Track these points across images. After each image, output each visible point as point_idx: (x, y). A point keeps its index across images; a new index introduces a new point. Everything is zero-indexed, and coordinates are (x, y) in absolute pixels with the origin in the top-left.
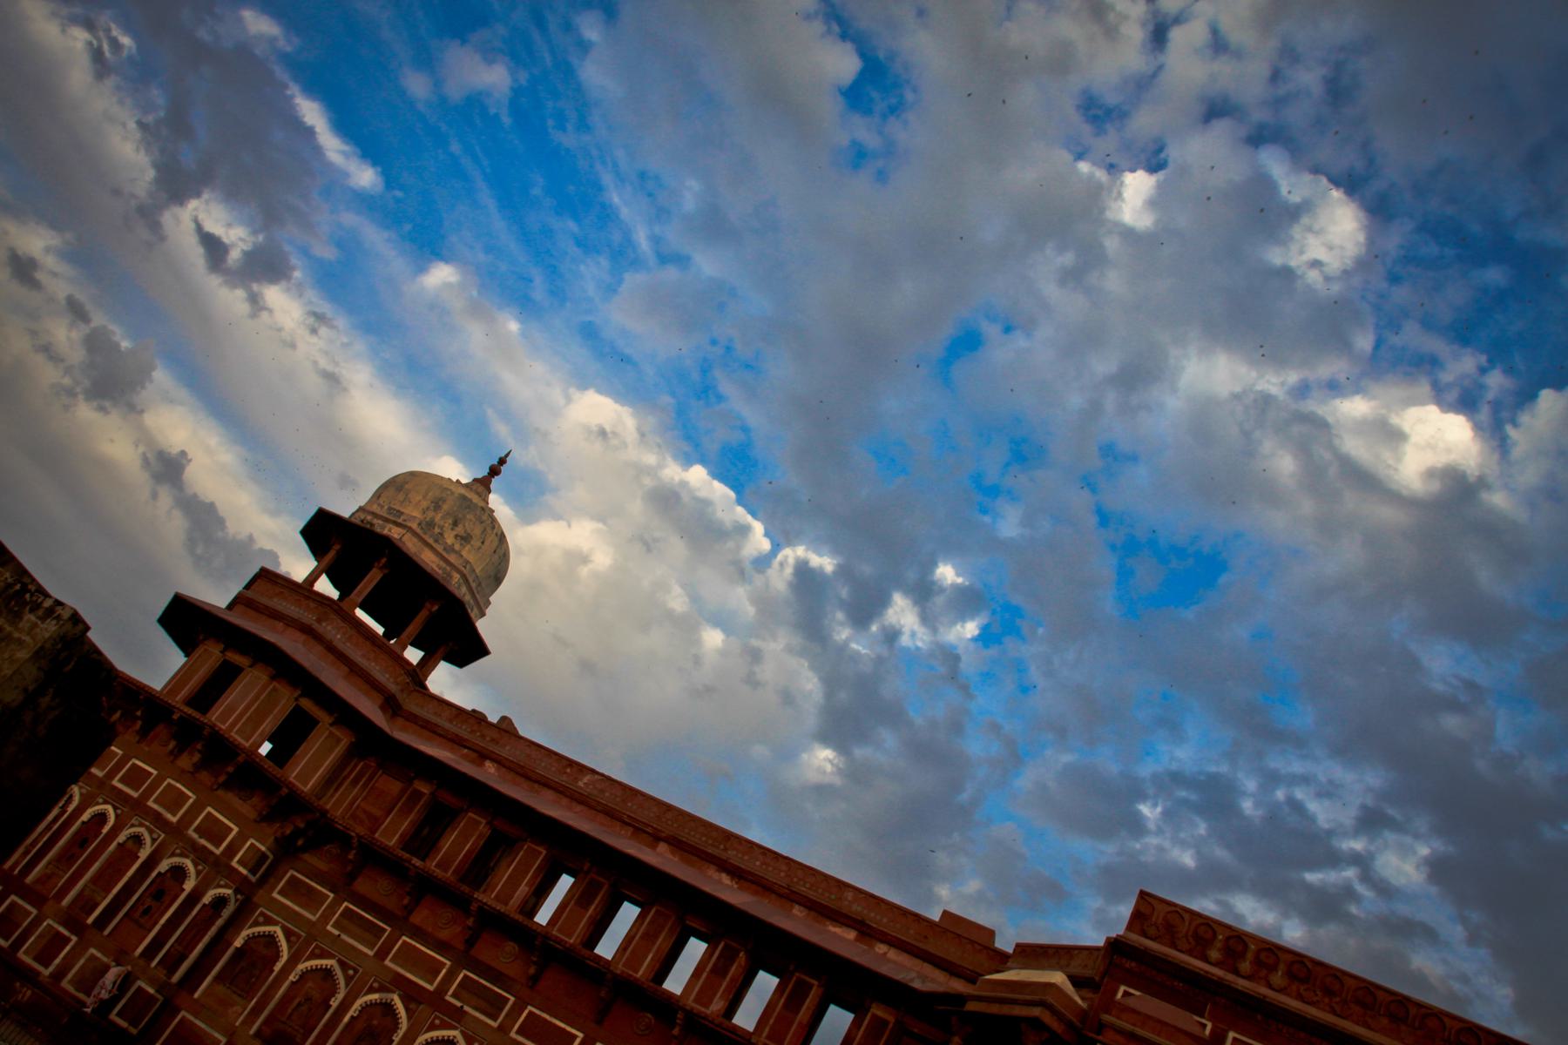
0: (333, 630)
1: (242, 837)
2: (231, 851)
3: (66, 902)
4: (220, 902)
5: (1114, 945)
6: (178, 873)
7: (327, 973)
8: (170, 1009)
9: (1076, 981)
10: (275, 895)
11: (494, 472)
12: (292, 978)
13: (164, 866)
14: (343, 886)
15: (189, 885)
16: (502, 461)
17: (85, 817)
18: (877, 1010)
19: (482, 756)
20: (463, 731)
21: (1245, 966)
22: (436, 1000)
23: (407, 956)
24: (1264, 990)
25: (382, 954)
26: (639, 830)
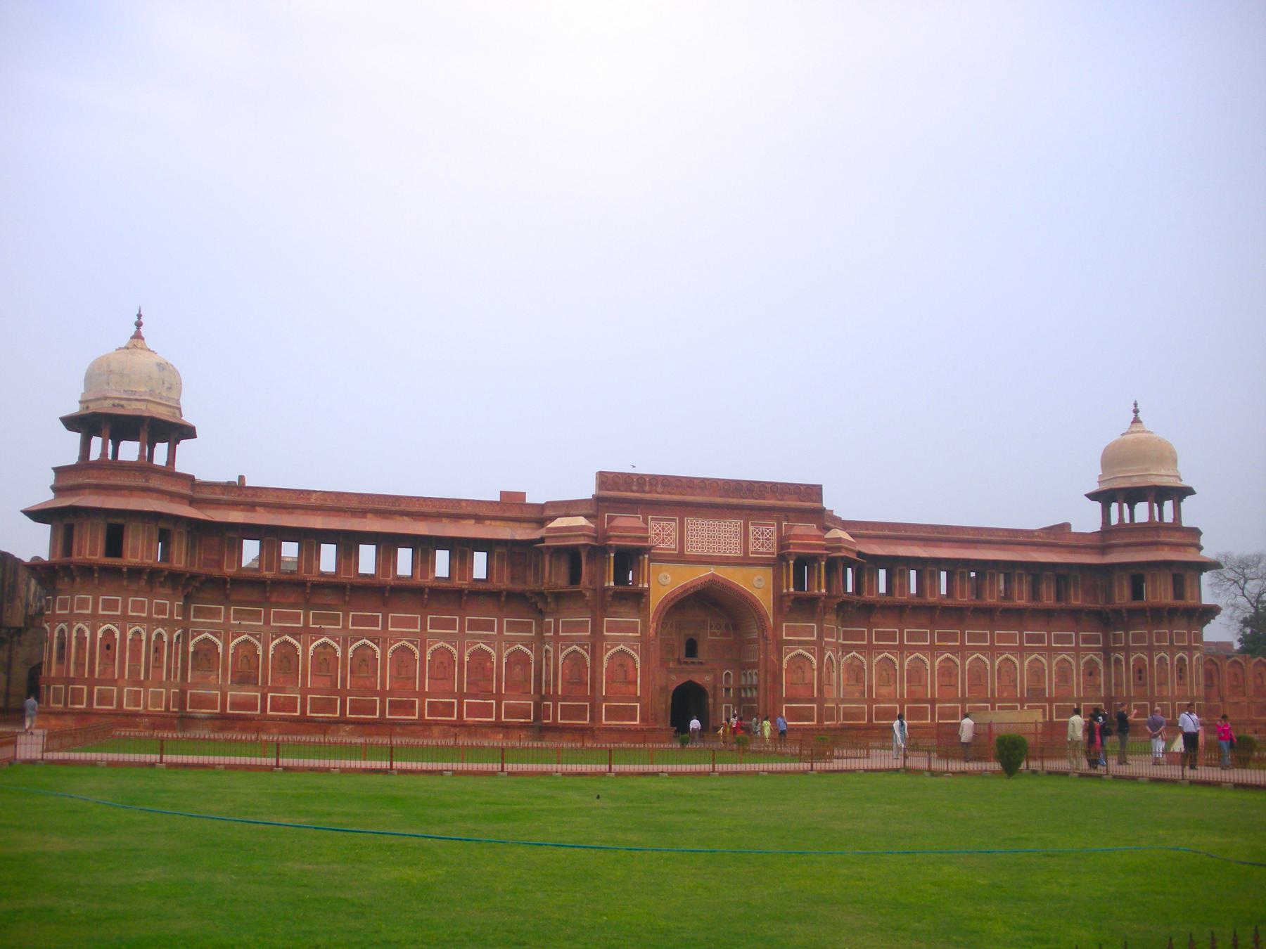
4: (178, 637)
5: (597, 499)
6: (160, 636)
7: (246, 641)
11: (139, 325)
12: (231, 652)
13: (153, 638)
14: (227, 600)
15: (166, 639)
16: (139, 316)
17: (100, 635)
18: (498, 550)
19: (252, 507)
21: (647, 488)
22: (306, 628)
23: (279, 617)
24: (655, 496)
25: (267, 622)
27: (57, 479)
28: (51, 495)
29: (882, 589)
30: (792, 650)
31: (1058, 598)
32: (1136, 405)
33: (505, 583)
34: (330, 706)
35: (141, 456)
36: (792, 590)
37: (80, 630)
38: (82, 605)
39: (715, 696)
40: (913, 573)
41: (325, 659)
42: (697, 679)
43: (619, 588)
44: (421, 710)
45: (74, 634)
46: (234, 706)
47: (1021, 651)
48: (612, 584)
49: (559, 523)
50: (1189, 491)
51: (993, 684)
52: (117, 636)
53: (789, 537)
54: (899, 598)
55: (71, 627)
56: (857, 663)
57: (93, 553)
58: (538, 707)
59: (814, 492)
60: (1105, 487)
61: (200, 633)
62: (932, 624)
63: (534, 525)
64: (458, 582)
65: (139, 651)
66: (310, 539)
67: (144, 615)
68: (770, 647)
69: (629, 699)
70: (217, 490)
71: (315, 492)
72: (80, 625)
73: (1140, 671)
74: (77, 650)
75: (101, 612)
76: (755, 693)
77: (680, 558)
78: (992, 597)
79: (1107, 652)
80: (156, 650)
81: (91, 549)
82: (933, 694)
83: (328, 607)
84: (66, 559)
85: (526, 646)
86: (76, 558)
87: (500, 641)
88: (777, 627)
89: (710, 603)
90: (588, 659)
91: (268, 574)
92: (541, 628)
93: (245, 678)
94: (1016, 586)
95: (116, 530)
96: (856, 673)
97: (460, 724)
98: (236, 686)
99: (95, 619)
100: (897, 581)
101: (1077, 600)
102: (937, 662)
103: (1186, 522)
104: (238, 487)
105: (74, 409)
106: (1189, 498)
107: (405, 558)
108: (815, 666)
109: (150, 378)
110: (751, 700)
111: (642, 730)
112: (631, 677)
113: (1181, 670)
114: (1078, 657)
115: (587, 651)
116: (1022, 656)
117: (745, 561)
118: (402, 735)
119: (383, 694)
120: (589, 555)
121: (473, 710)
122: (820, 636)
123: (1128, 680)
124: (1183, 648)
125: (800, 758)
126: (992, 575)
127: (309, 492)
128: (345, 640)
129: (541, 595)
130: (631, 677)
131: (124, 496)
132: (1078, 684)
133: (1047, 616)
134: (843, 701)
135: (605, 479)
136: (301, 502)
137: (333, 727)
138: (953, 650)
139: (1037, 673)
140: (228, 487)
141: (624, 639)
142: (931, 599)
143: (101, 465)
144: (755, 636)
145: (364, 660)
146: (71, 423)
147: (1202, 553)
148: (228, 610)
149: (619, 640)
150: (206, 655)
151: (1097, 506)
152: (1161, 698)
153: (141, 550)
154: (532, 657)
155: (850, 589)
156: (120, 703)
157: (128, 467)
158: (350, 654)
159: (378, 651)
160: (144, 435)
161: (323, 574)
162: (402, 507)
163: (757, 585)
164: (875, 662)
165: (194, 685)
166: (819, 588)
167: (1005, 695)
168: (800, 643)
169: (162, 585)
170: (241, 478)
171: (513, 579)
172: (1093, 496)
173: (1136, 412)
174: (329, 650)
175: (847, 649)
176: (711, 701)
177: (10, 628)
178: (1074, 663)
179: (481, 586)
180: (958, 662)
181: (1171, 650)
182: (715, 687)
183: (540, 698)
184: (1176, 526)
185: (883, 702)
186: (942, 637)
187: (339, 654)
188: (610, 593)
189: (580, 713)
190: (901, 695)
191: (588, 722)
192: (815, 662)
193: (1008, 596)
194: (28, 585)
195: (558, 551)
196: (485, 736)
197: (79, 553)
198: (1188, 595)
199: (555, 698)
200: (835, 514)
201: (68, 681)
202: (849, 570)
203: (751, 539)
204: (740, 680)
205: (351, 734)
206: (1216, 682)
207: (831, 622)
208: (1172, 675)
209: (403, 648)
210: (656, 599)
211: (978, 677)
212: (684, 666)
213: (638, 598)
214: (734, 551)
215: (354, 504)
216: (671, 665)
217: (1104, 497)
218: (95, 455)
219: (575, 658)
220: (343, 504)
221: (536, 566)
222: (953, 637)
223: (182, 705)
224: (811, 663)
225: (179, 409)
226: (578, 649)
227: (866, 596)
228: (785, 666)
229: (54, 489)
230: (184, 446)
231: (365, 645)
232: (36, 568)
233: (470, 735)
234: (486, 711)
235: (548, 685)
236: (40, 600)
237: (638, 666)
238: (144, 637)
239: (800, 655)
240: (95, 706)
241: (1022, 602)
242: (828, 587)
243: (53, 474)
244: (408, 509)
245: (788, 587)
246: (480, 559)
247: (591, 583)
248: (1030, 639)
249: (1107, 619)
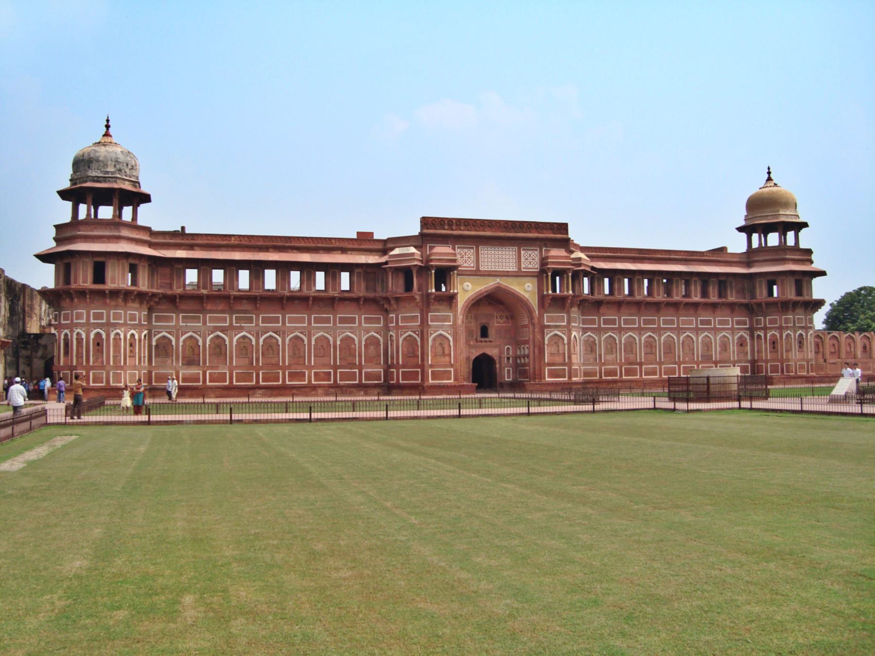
0: (125, 233)
1: (140, 314)
2: (140, 320)
3: (112, 364)
5: (421, 235)
6: (133, 335)
7: (191, 337)
8: (150, 373)
9: (415, 247)
10: (154, 324)
11: (108, 127)
12: (181, 344)
13: (128, 337)
14: (176, 309)
15: (137, 337)
16: (108, 121)
17: (92, 336)
18: (357, 270)
19: (191, 247)
20: (178, 241)
21: (454, 227)
22: (231, 326)
23: (212, 320)
25: (205, 323)
26: (261, 249)
27: (57, 234)
28: (54, 244)
29: (607, 292)
30: (551, 332)
31: (720, 296)
32: (769, 168)
33: (361, 292)
34: (247, 377)
35: (114, 216)
36: (550, 292)
37: (78, 334)
38: (79, 316)
40: (626, 280)
41: (244, 347)
43: (438, 293)
44: (310, 378)
45: (75, 336)
46: (184, 380)
47: (697, 330)
48: (434, 290)
49: (397, 251)
50: (805, 225)
51: (679, 351)
52: (104, 336)
53: (547, 258)
54: (617, 297)
55: (72, 332)
56: (591, 339)
57: (85, 281)
58: (384, 371)
59: (563, 228)
60: (750, 223)
61: (159, 332)
62: (639, 313)
63: (380, 253)
64: (331, 293)
65: (120, 346)
66: (231, 267)
67: (122, 322)
68: (536, 330)
69: (445, 366)
70: (167, 236)
71: (234, 235)
72: (79, 330)
73: (774, 343)
74: (77, 347)
75: (92, 321)
76: (527, 360)
77: (477, 273)
78: (677, 295)
79: (751, 330)
80: (131, 345)
81: (84, 279)
82: (641, 359)
83: (245, 312)
84: (66, 287)
85: (377, 333)
86: (73, 286)
87: (361, 330)
88: (541, 316)
89: (494, 301)
90: (419, 340)
91: (204, 292)
92: (387, 321)
93: (190, 362)
94: (693, 288)
95: (99, 265)
96: (591, 347)
97: (335, 386)
98: (185, 367)
99: (88, 326)
100: (616, 286)
101: (732, 298)
102: (643, 338)
103: (803, 245)
104: (181, 234)
105: (66, 185)
106: (804, 231)
107: (295, 277)
108: (566, 342)
109: (117, 161)
110: (524, 365)
111: (455, 386)
113: (800, 342)
114: (733, 334)
115: (418, 335)
116: (697, 334)
117: (519, 274)
118: (298, 395)
119: (284, 368)
120: (417, 272)
121: (344, 376)
122: (569, 322)
123: (766, 350)
124: (802, 328)
125: (576, 402)
126: (677, 281)
127: (230, 236)
128: (257, 334)
129: (387, 299)
130: (447, 351)
131: (104, 242)
132: (734, 352)
133: (714, 306)
134: (584, 364)
135: (426, 222)
136: (226, 242)
137: (251, 392)
138: (653, 330)
139: (707, 345)
140: (174, 234)
141: (441, 327)
142: (638, 298)
143: (87, 222)
144: (526, 322)
145: (271, 347)
146: (64, 194)
147: (813, 265)
148: (178, 316)
150: (163, 349)
151: (744, 236)
152: (788, 360)
153: (119, 278)
154: (381, 340)
155: (586, 290)
156: (108, 381)
157: (105, 223)
158: (261, 343)
159: (280, 340)
160: (116, 201)
161: (240, 291)
162: (293, 244)
163: (527, 290)
164: (603, 339)
165: (156, 367)
166: (568, 291)
167: (687, 359)
168: (556, 327)
169: (133, 301)
170: (183, 228)
171: (367, 289)
172: (740, 229)
173: (769, 173)
174: (246, 340)
175: (585, 330)
176: (498, 366)
177: (30, 334)
178: (730, 338)
179: (346, 295)
180: (657, 338)
181: (795, 329)
182: (500, 357)
183: (388, 367)
184: (796, 248)
185: (609, 365)
186: (646, 322)
187: (254, 343)
188: (433, 297)
189: (414, 375)
190: (621, 360)
191: (419, 382)
193: (687, 295)
194: (40, 306)
195: (397, 270)
196: (351, 394)
197: (75, 282)
198: (805, 293)
199: (397, 367)
200: (575, 242)
201: (72, 368)
202: (586, 280)
203: (523, 259)
204: (516, 352)
205: (264, 395)
206: (821, 350)
207: (575, 312)
208: (795, 345)
209: (297, 337)
210: (462, 301)
211: (669, 348)
213: (450, 300)
214: (513, 268)
215: (260, 243)
216: (472, 343)
217: (747, 229)
218: (82, 215)
219: (410, 340)
220: (253, 243)
221: (383, 281)
222: (652, 322)
223: (150, 381)
224: (563, 339)
225: (139, 183)
226: (412, 334)
227: (597, 296)
228: (546, 342)
229: (58, 240)
230: (143, 208)
231: (271, 336)
232: (45, 293)
233: (344, 393)
234: (352, 376)
235: (392, 358)
236: (49, 316)
237: (452, 344)
238: (122, 337)
239: (556, 335)
240: (91, 384)
241: (697, 298)
242: (573, 291)
243: (54, 230)
244: (296, 245)
245: (547, 290)
246: (345, 277)
247: (419, 290)
248: (702, 322)
249: (751, 309)
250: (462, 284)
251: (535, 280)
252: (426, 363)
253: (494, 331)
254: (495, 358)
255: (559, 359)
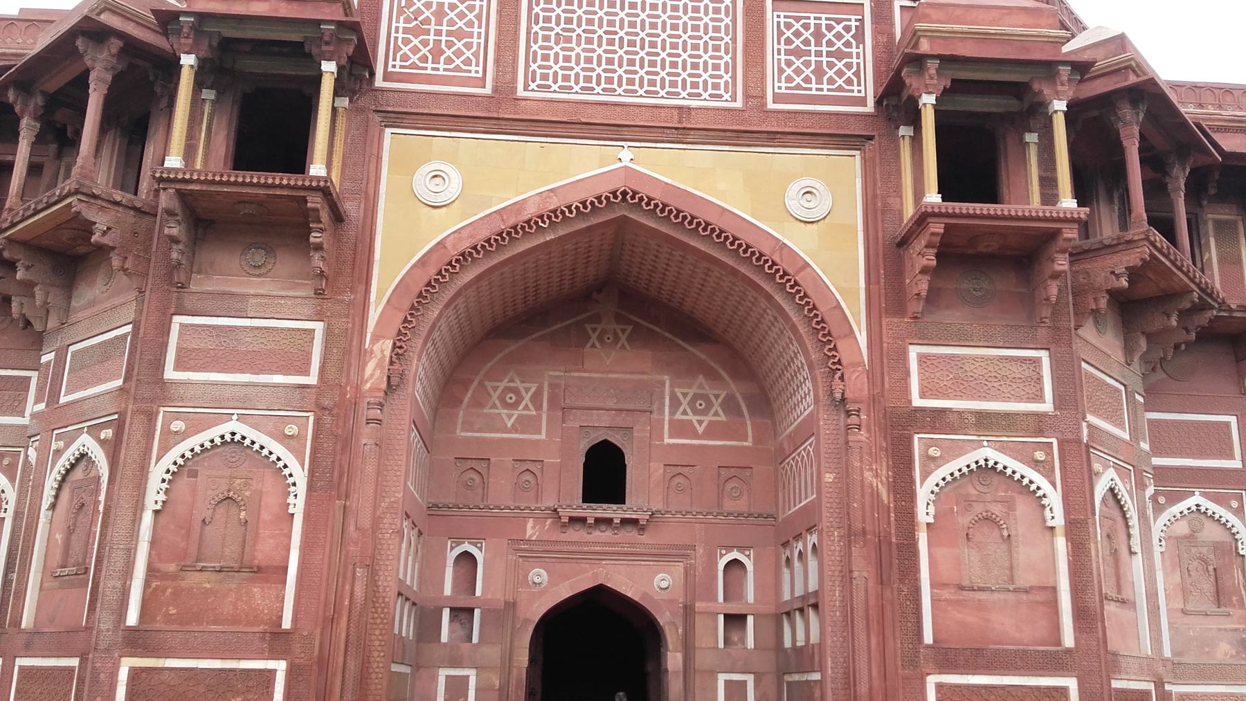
36: (933, 197)
39: (688, 648)
42: (627, 581)
56: (1211, 533)
88: (888, 360)
108: (1057, 518)
112: (264, 551)
141: (243, 400)
149: (224, 401)
168: (985, 422)
175: (1174, 484)
176: (673, 660)
182: (688, 612)
192: (1054, 499)
212: (576, 534)
224: (1038, 500)
228: (924, 513)
239: (987, 471)
250: (408, 166)
251: (851, 164)
252: (105, 622)
253: (657, 470)
254: (663, 618)
255: (1010, 625)
